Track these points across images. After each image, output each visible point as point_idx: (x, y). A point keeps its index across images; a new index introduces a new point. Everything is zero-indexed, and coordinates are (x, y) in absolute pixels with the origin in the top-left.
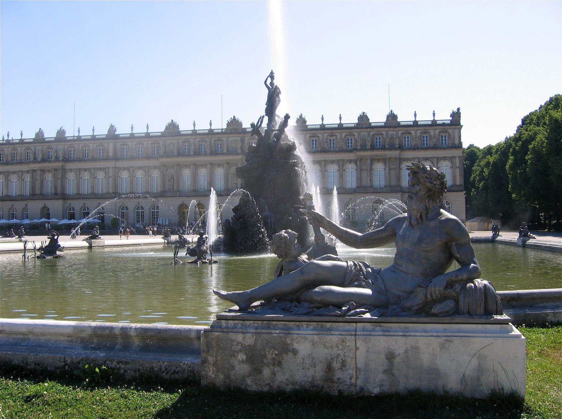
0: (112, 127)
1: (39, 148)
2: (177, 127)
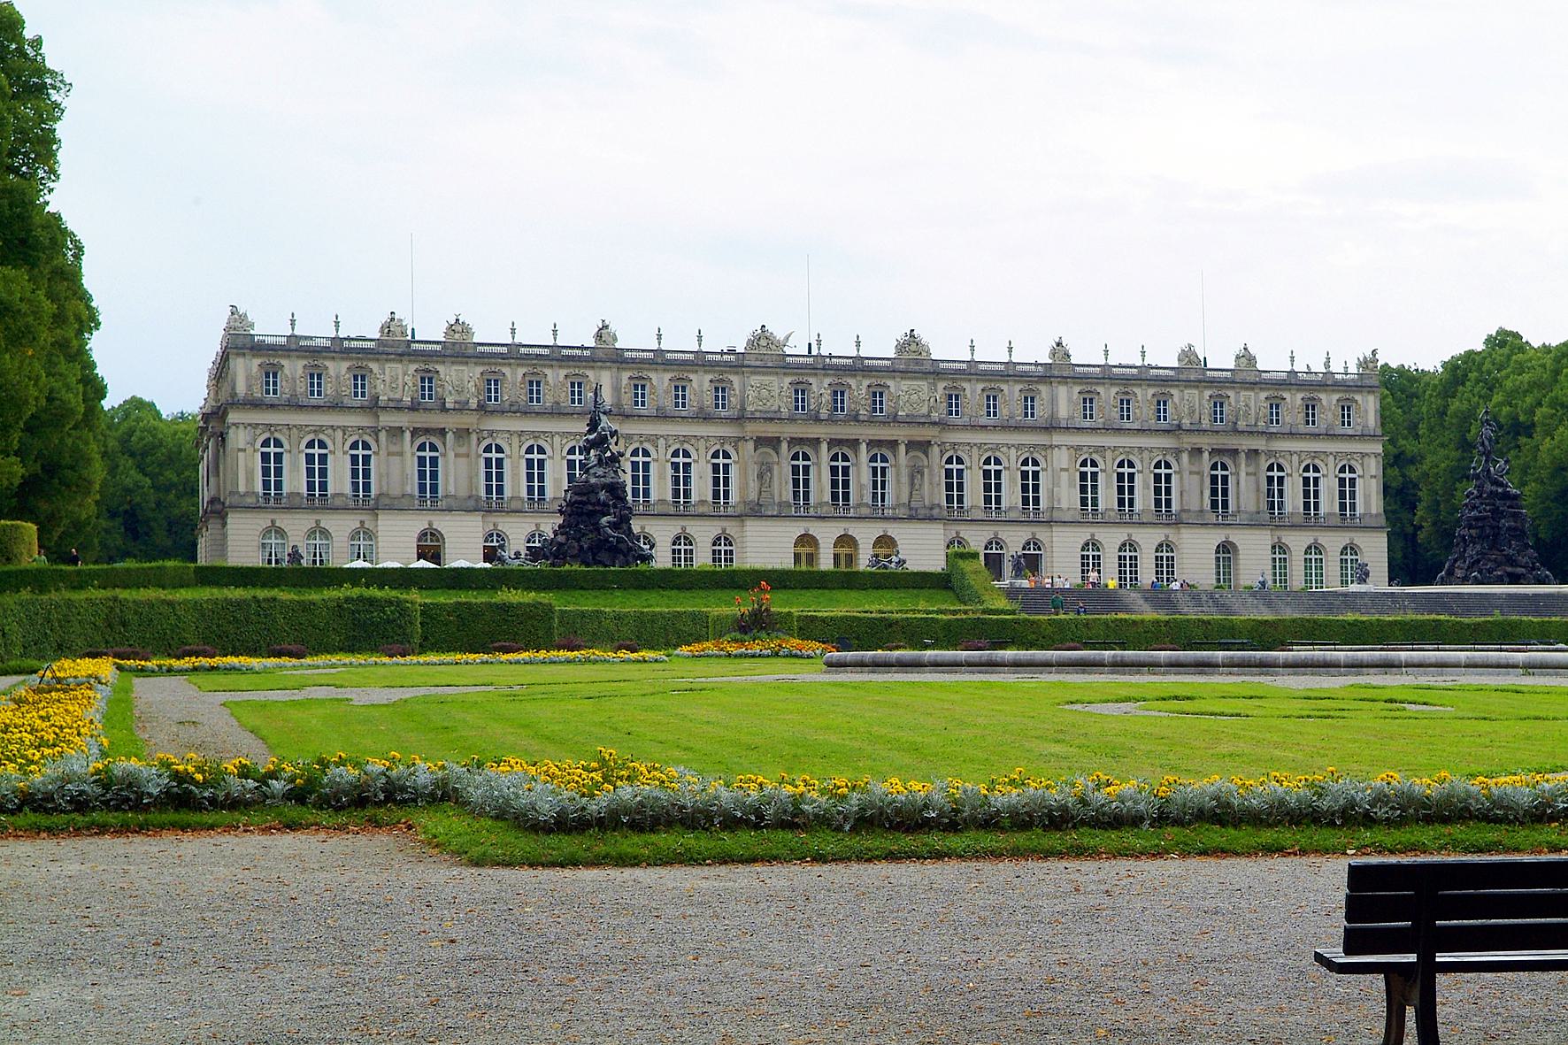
1: (394, 369)
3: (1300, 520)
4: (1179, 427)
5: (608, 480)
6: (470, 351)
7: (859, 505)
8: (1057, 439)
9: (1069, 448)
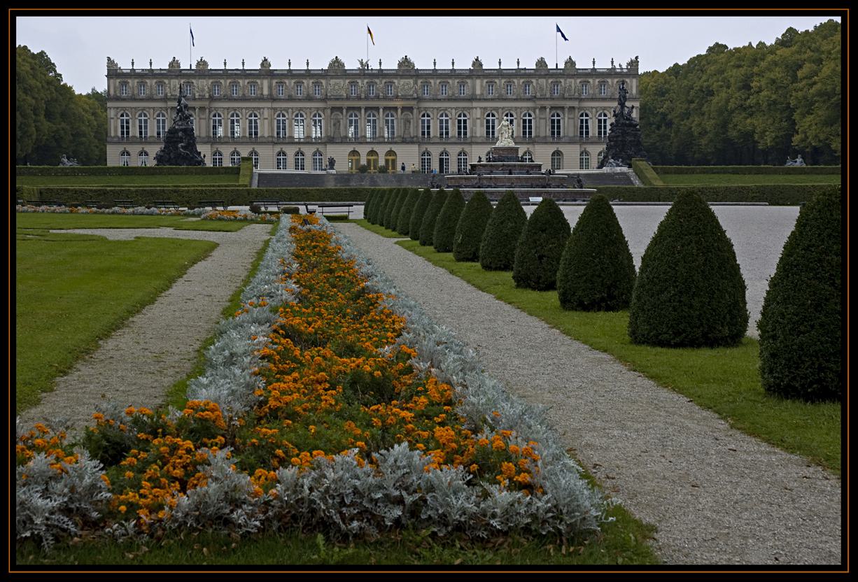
0: (266, 60)
2: (343, 65)
3: (596, 140)
4: (535, 97)
5: (184, 127)
6: (206, 73)
7: (452, 137)
8: (475, 104)
9: (481, 108)
